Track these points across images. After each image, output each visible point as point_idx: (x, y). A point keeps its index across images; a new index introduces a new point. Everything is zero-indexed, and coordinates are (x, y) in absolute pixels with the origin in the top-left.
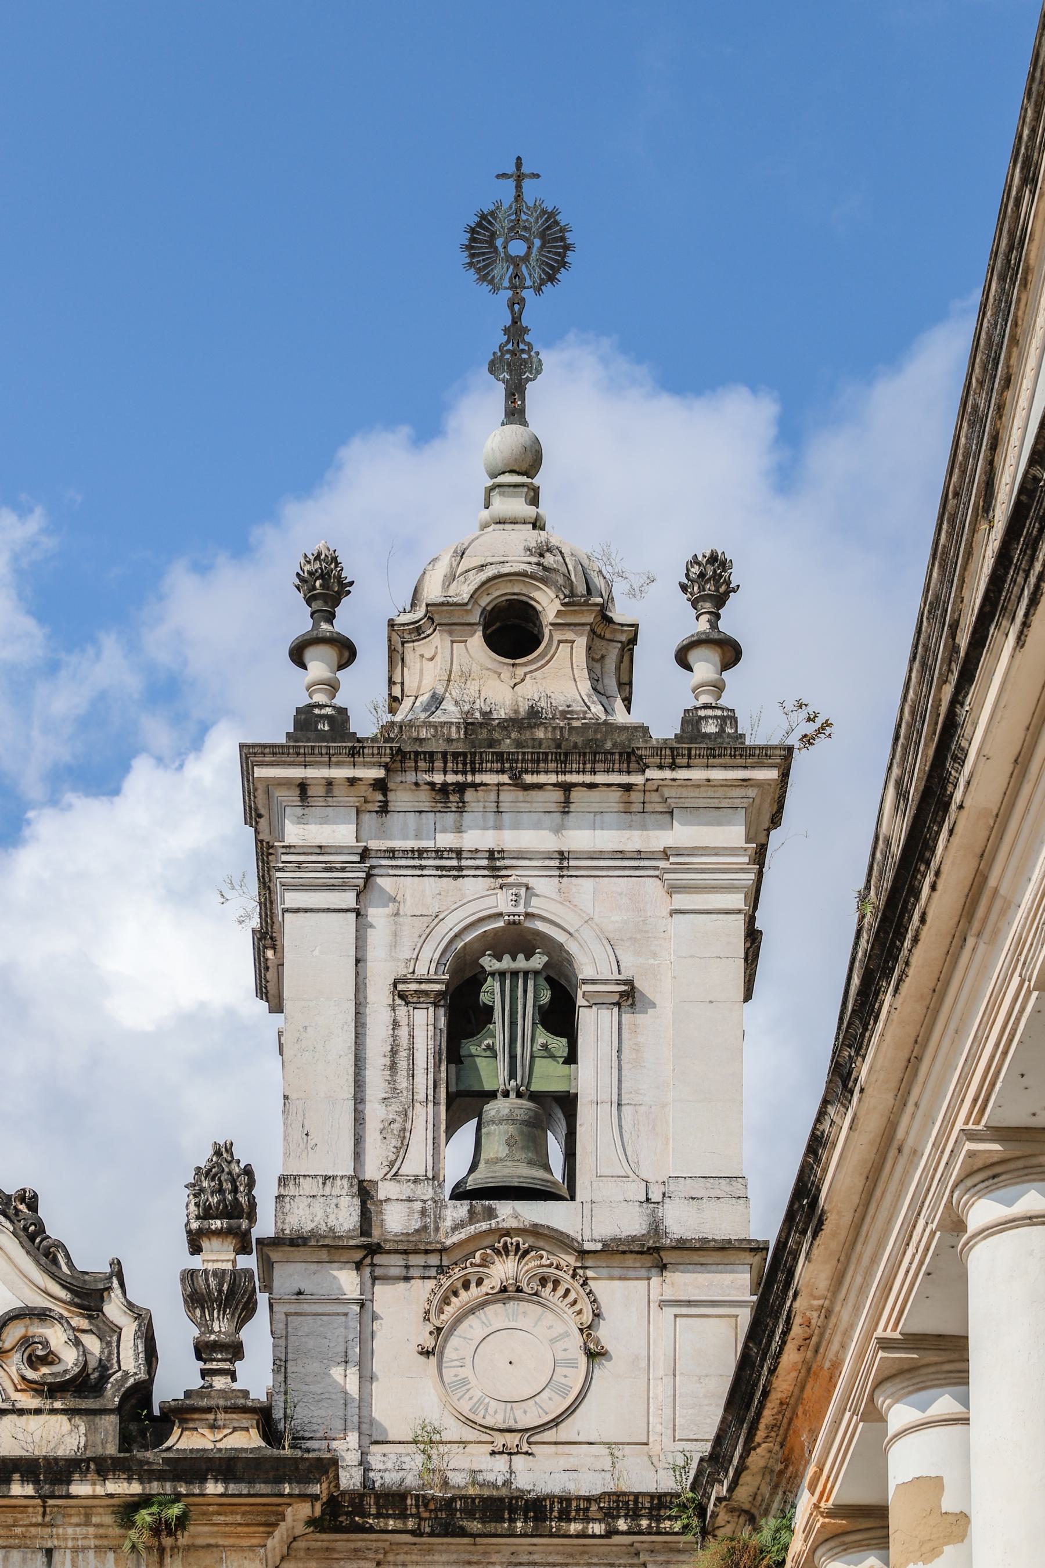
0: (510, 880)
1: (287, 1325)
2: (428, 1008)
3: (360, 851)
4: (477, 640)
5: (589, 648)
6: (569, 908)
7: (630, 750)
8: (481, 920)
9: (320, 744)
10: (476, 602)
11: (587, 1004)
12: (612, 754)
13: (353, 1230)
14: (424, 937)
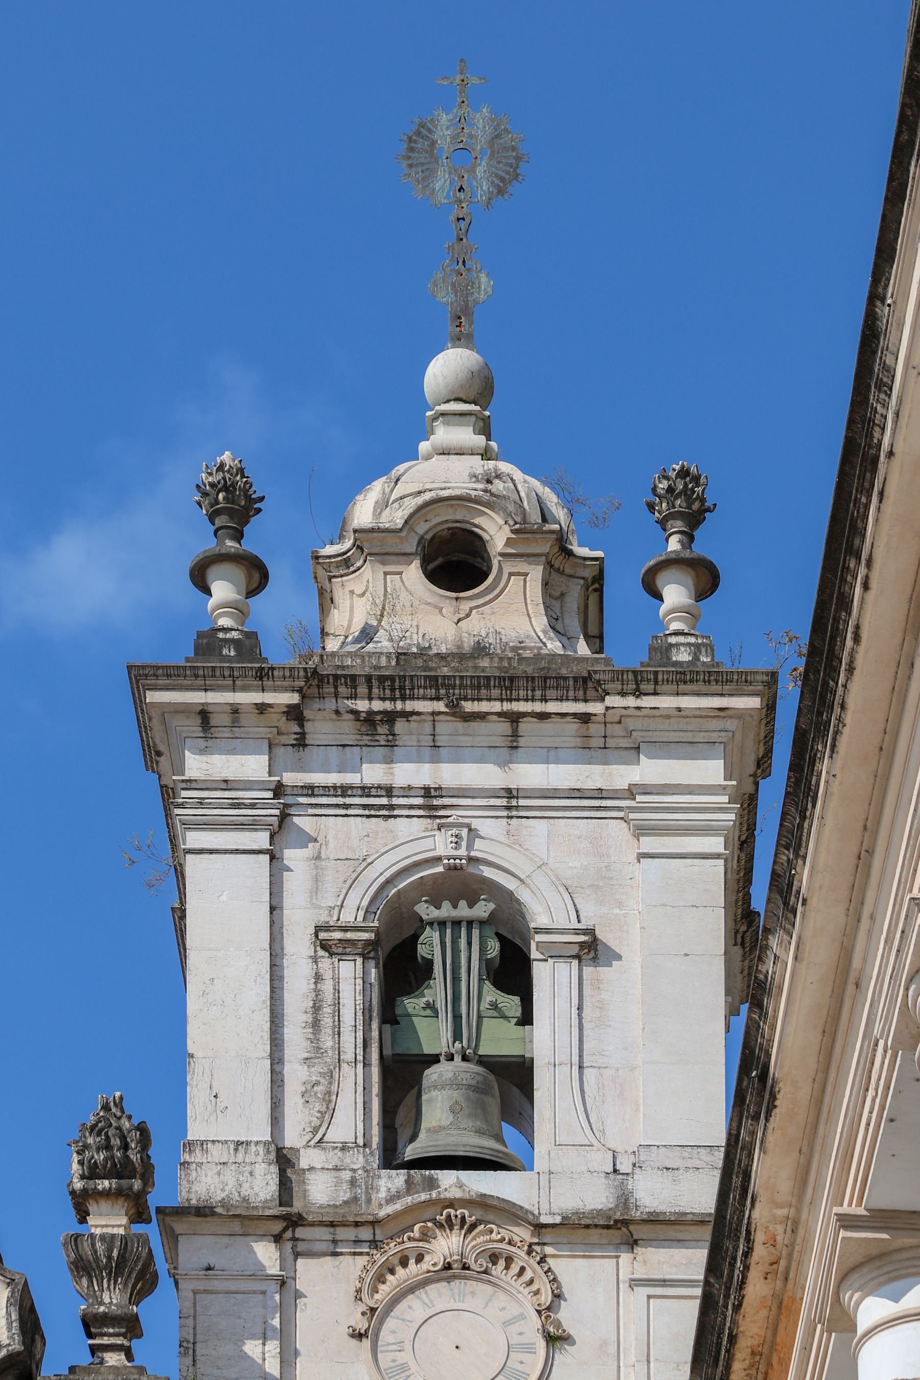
2: (355, 960)
4: (413, 573)
5: (546, 584)
10: (412, 529)
11: (542, 957)
12: (565, 678)
14: (349, 882)
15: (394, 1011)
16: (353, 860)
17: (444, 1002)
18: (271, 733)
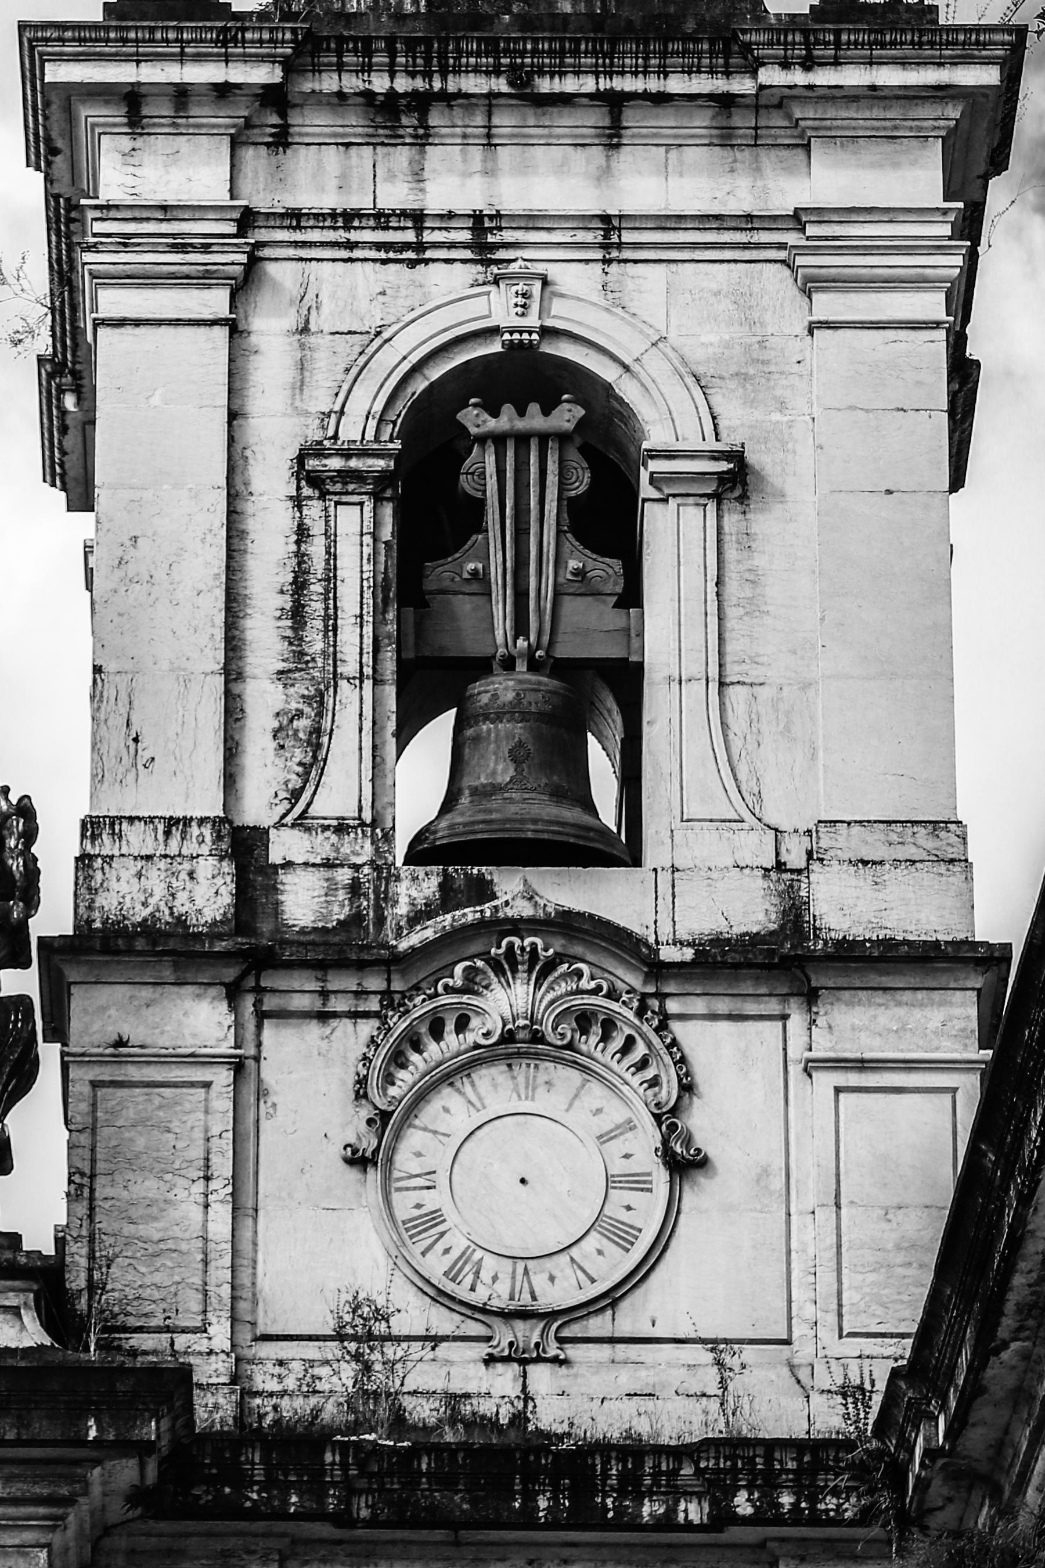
0: (514, 267)
1: (94, 1105)
2: (361, 504)
3: (236, 215)
6: (623, 319)
7: (728, 35)
9: (165, 24)
13: (221, 921)
14: (354, 371)
15: (421, 584)
16: (361, 333)
17: (500, 571)
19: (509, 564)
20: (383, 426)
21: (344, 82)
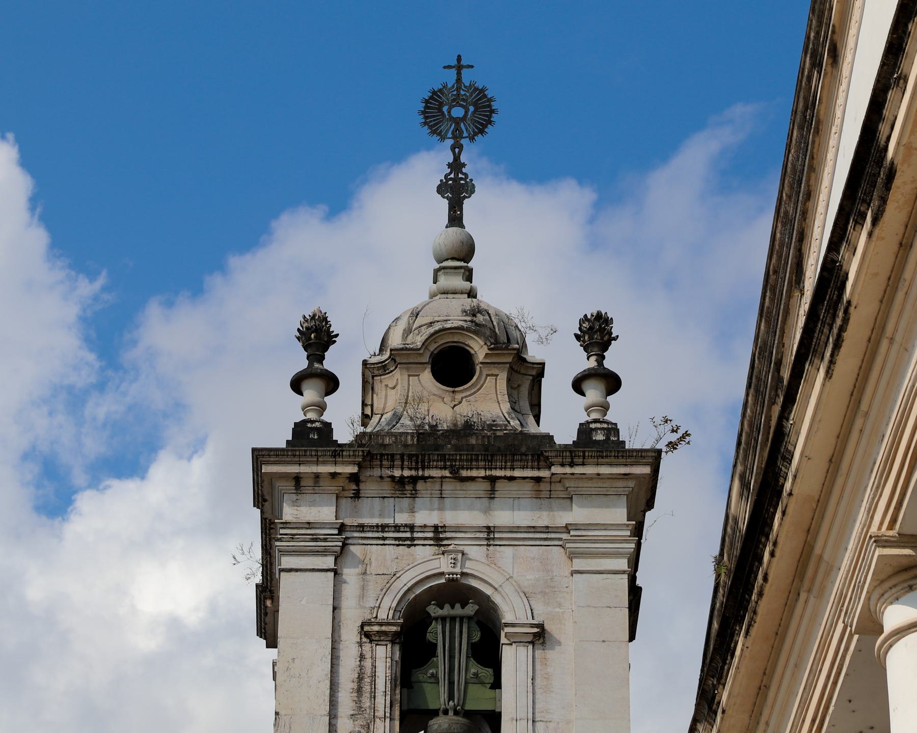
2: (386, 645)
3: (338, 526)
6: (495, 569)
8: (428, 578)
14: (385, 590)
16: (387, 575)
17: (443, 673)
18: (338, 490)
19: (446, 670)
20: (396, 613)
21: (383, 472)
